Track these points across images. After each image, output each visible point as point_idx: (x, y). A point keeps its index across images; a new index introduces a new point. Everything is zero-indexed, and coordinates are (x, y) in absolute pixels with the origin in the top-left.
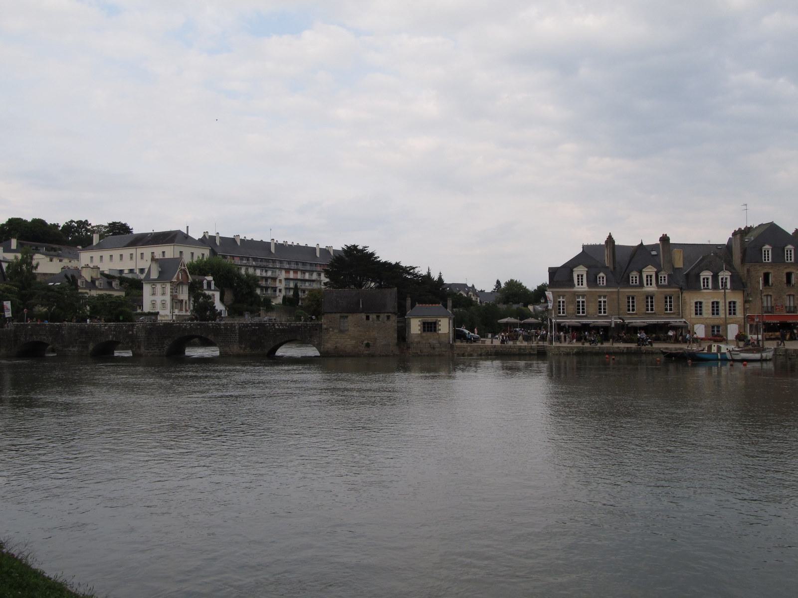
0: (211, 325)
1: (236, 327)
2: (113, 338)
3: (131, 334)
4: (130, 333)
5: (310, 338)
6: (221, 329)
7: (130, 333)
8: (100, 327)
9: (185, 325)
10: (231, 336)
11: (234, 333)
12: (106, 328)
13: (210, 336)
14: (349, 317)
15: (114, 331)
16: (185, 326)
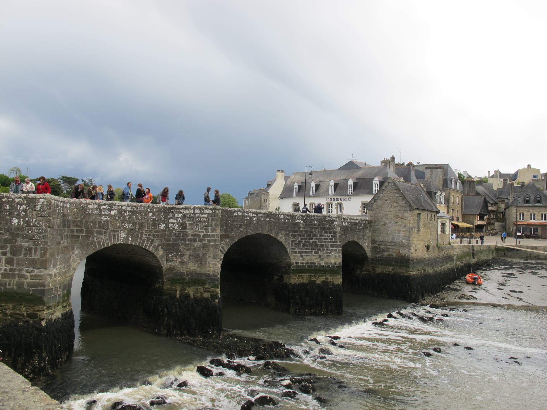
0: (282, 216)
1: (335, 223)
2: (127, 237)
3: (163, 231)
4: (162, 226)
5: (363, 238)
6: (295, 224)
7: (162, 226)
8: (100, 211)
9: (250, 214)
10: (321, 236)
11: (331, 233)
12: (113, 213)
13: (280, 235)
14: (421, 215)
15: (129, 222)
16: (251, 217)
